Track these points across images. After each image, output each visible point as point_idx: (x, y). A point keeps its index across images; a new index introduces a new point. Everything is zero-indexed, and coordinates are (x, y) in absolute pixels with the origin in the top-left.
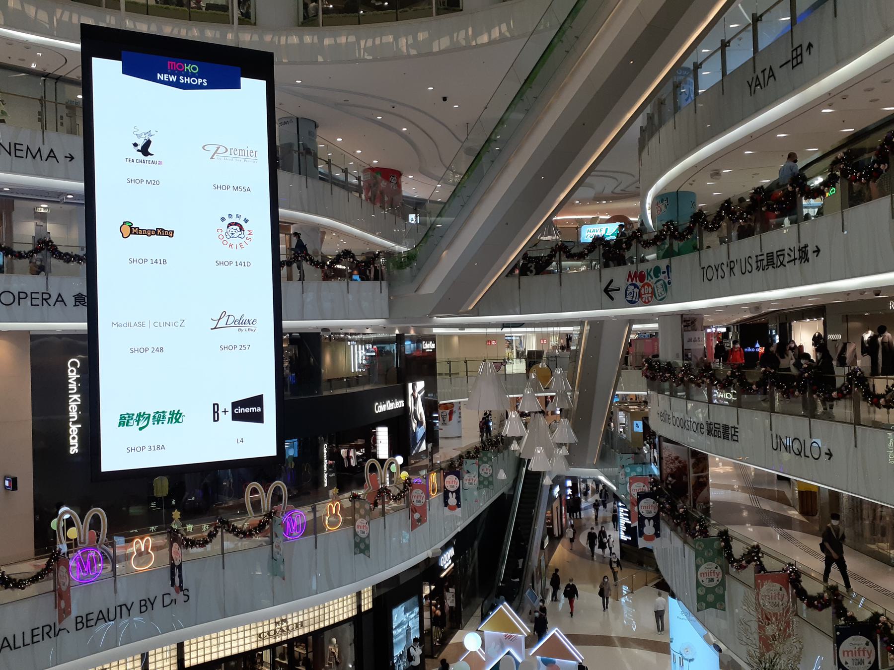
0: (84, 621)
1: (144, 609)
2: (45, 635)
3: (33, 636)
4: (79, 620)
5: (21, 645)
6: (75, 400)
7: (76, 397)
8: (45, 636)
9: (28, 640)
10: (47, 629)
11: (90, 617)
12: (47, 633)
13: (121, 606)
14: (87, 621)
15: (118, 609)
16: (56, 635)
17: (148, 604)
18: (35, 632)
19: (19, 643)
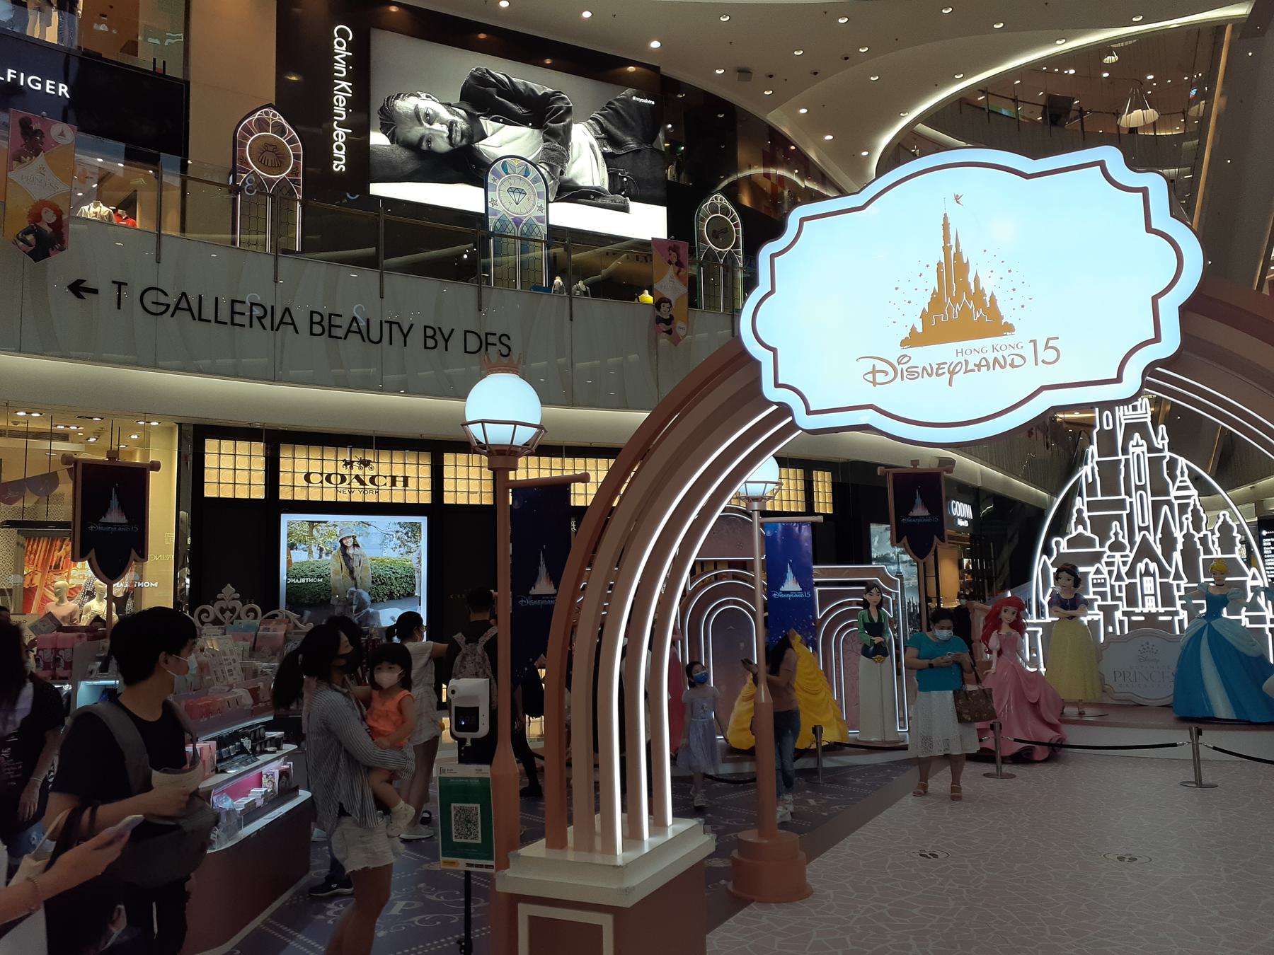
0: (326, 323)
1: (431, 343)
2: (255, 321)
3: (233, 313)
4: (317, 318)
5: (213, 320)
6: (343, 90)
7: (344, 84)
8: (255, 321)
9: (224, 314)
10: (257, 312)
11: (336, 321)
12: (260, 319)
13: (391, 323)
14: (331, 326)
15: (386, 326)
16: (275, 328)
17: (438, 337)
18: (238, 307)
19: (208, 312)
